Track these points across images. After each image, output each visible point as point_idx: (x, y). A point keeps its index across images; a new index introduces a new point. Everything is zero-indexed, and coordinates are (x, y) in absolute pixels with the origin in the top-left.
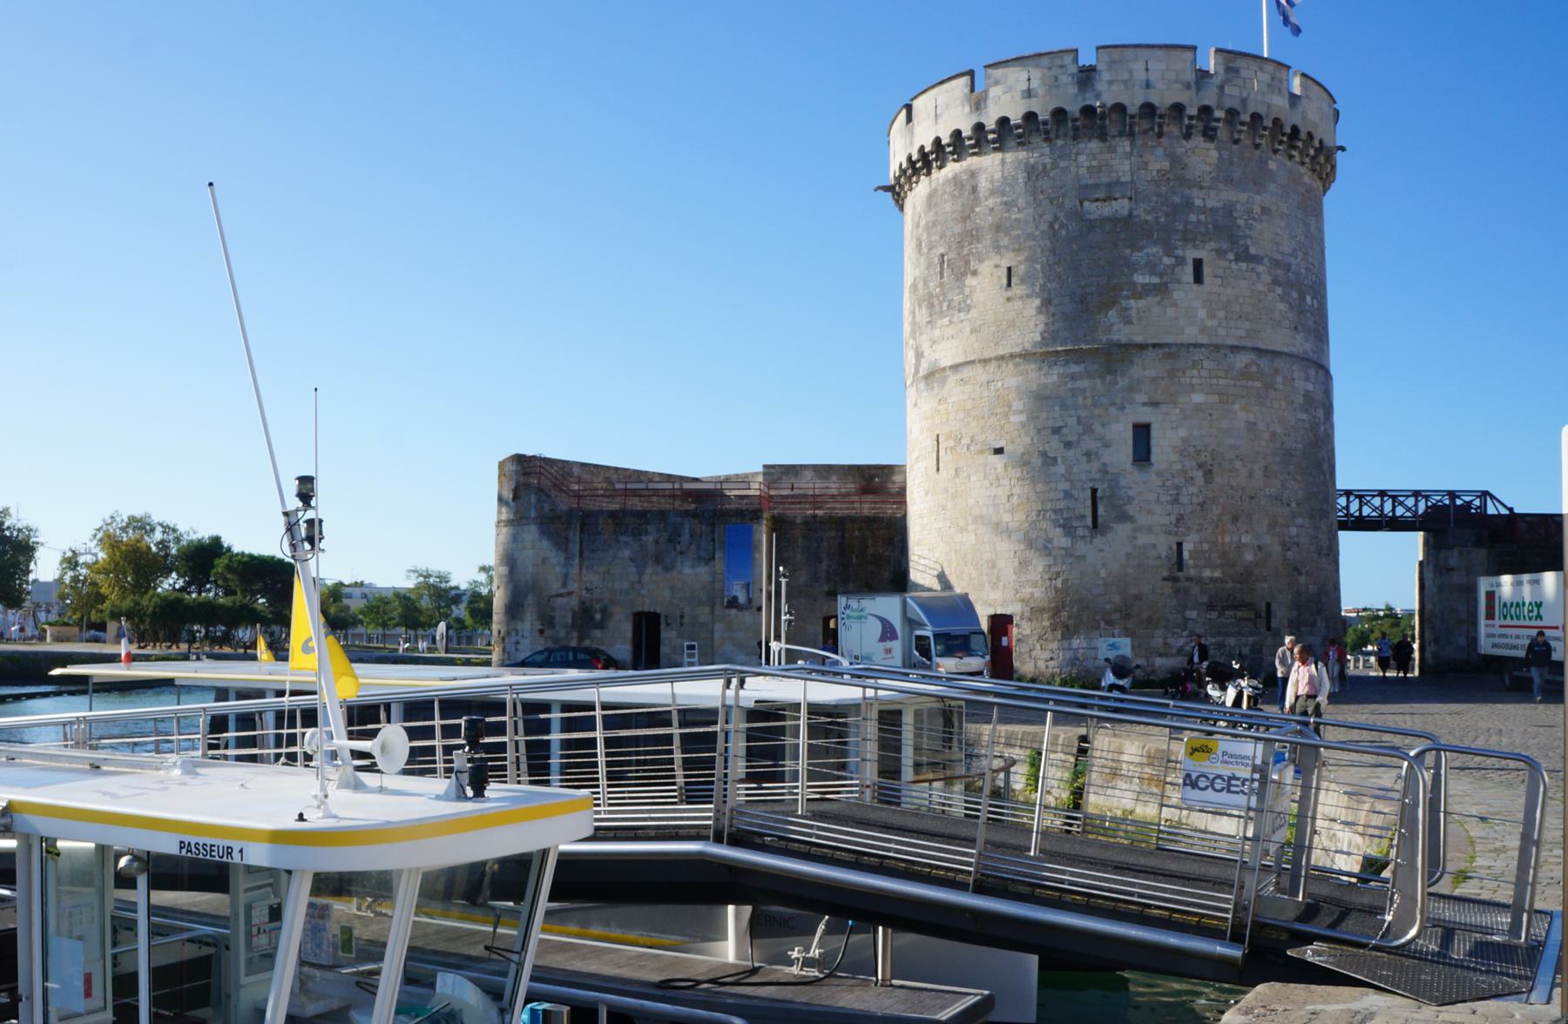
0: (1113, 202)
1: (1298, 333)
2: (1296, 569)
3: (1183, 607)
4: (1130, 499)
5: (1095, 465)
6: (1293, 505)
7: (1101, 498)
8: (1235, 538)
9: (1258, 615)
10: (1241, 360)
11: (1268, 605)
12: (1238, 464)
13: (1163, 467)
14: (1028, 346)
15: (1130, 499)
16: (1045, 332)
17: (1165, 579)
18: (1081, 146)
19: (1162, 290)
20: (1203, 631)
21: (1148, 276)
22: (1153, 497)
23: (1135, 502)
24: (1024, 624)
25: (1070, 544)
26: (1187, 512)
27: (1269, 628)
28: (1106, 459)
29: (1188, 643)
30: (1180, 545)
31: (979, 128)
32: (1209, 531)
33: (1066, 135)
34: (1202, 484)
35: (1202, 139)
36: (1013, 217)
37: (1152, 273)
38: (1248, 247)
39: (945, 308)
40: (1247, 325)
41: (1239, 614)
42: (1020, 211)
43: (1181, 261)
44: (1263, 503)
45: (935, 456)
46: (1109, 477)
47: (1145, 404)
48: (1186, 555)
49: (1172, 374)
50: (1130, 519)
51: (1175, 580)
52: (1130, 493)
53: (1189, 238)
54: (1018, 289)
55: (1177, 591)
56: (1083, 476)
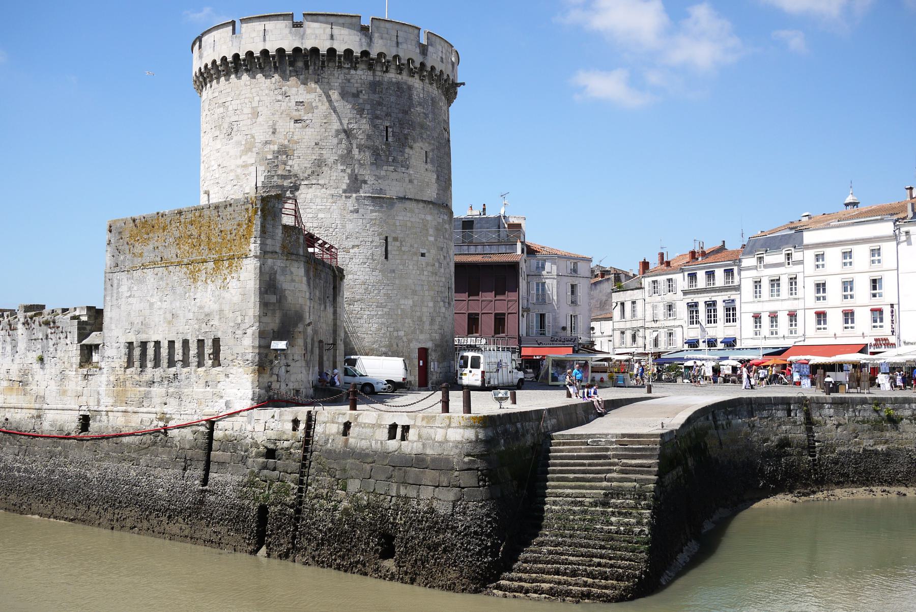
24: (433, 353)
31: (423, 65)
39: (390, 159)
45: (384, 249)
54: (429, 166)
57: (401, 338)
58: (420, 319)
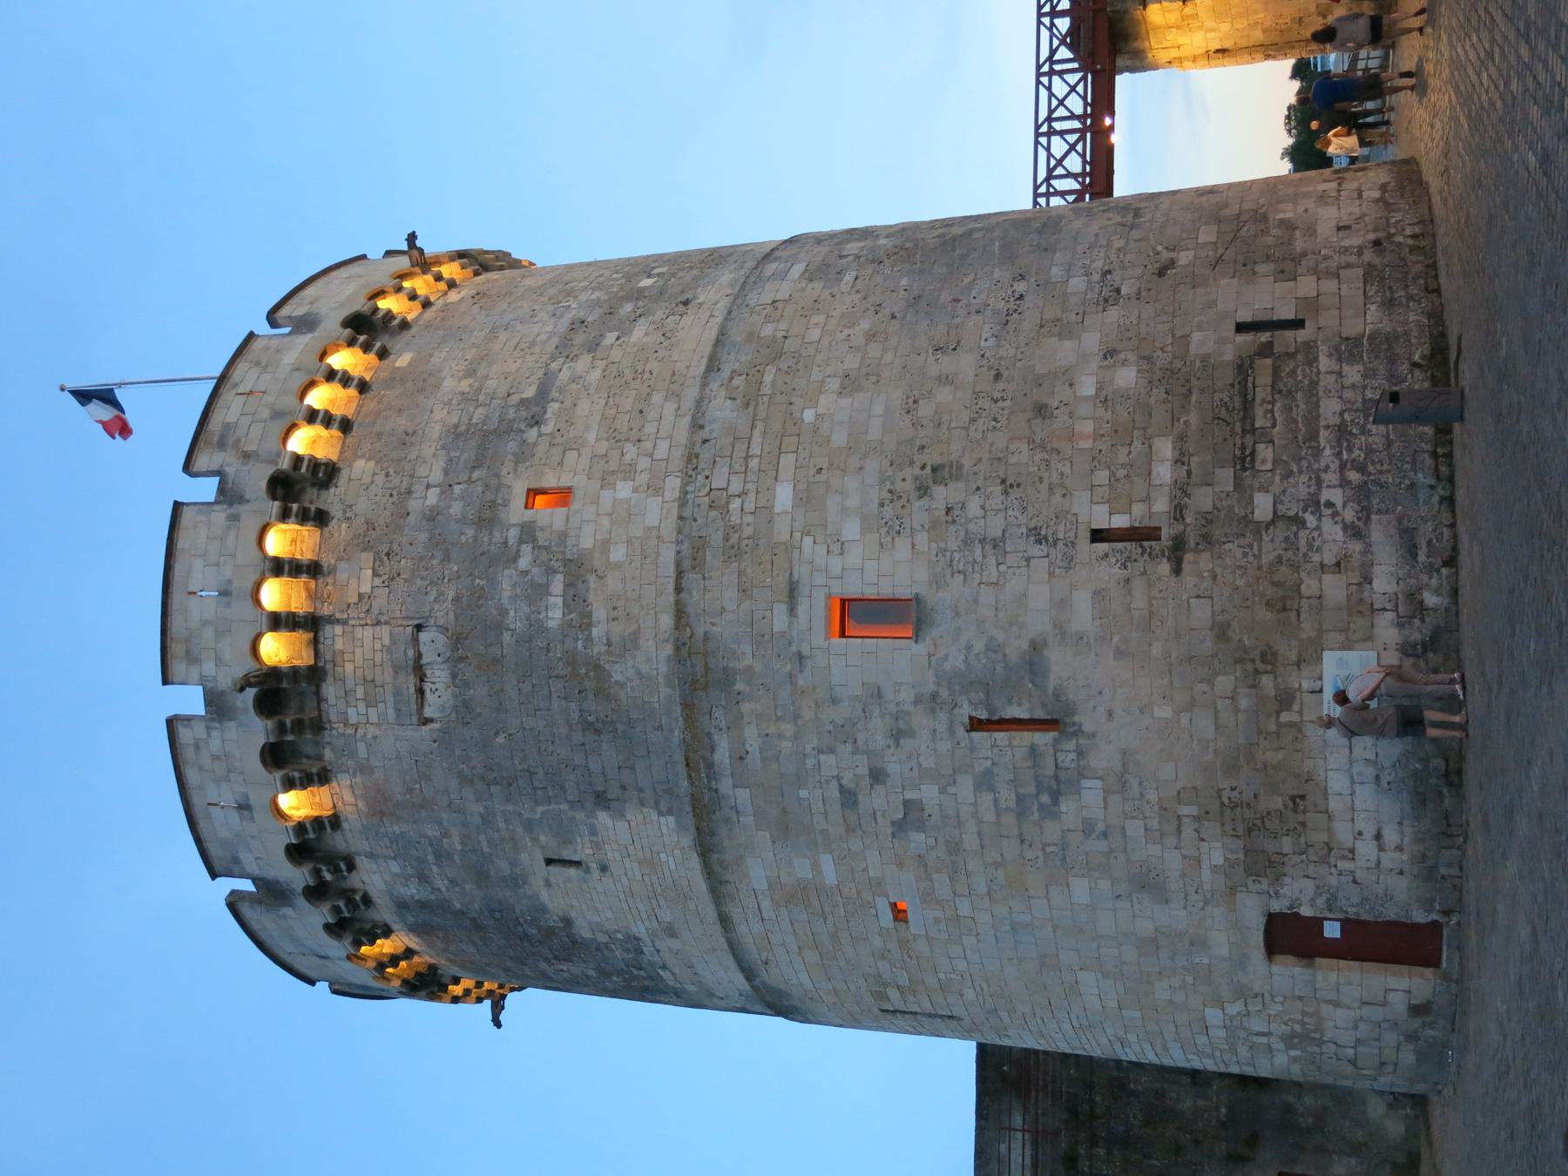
0: (424, 661)
1: (695, 297)
2: (1161, 273)
3: (1248, 526)
4: (992, 648)
5: (920, 721)
6: (1020, 287)
7: (990, 710)
8: (1084, 409)
9: (1266, 350)
10: (722, 410)
11: (1241, 328)
12: (925, 410)
13: (922, 574)
14: (687, 840)
15: (992, 648)
16: (657, 806)
17: (1177, 570)
18: (333, 718)
19: (577, 570)
20: (1304, 478)
21: (552, 599)
22: (987, 596)
23: (1000, 636)
25: (1098, 783)
26: (1023, 519)
27: (1298, 324)
28: (907, 696)
29: (1335, 514)
30: (1098, 536)
32: (1067, 470)
33: (317, 744)
34: (961, 485)
35: (332, 490)
36: (459, 847)
37: (542, 590)
38: (523, 401)
40: (657, 398)
41: (1262, 393)
42: (446, 835)
43: (528, 532)
44: (1011, 352)
46: (944, 693)
47: (792, 610)
48: (1120, 521)
49: (733, 552)
50: (1037, 646)
51: (1178, 549)
52: (979, 646)
53: (487, 516)
55: (1207, 540)
56: (944, 746)
57: (1232, 1018)
58: (1152, 944)
